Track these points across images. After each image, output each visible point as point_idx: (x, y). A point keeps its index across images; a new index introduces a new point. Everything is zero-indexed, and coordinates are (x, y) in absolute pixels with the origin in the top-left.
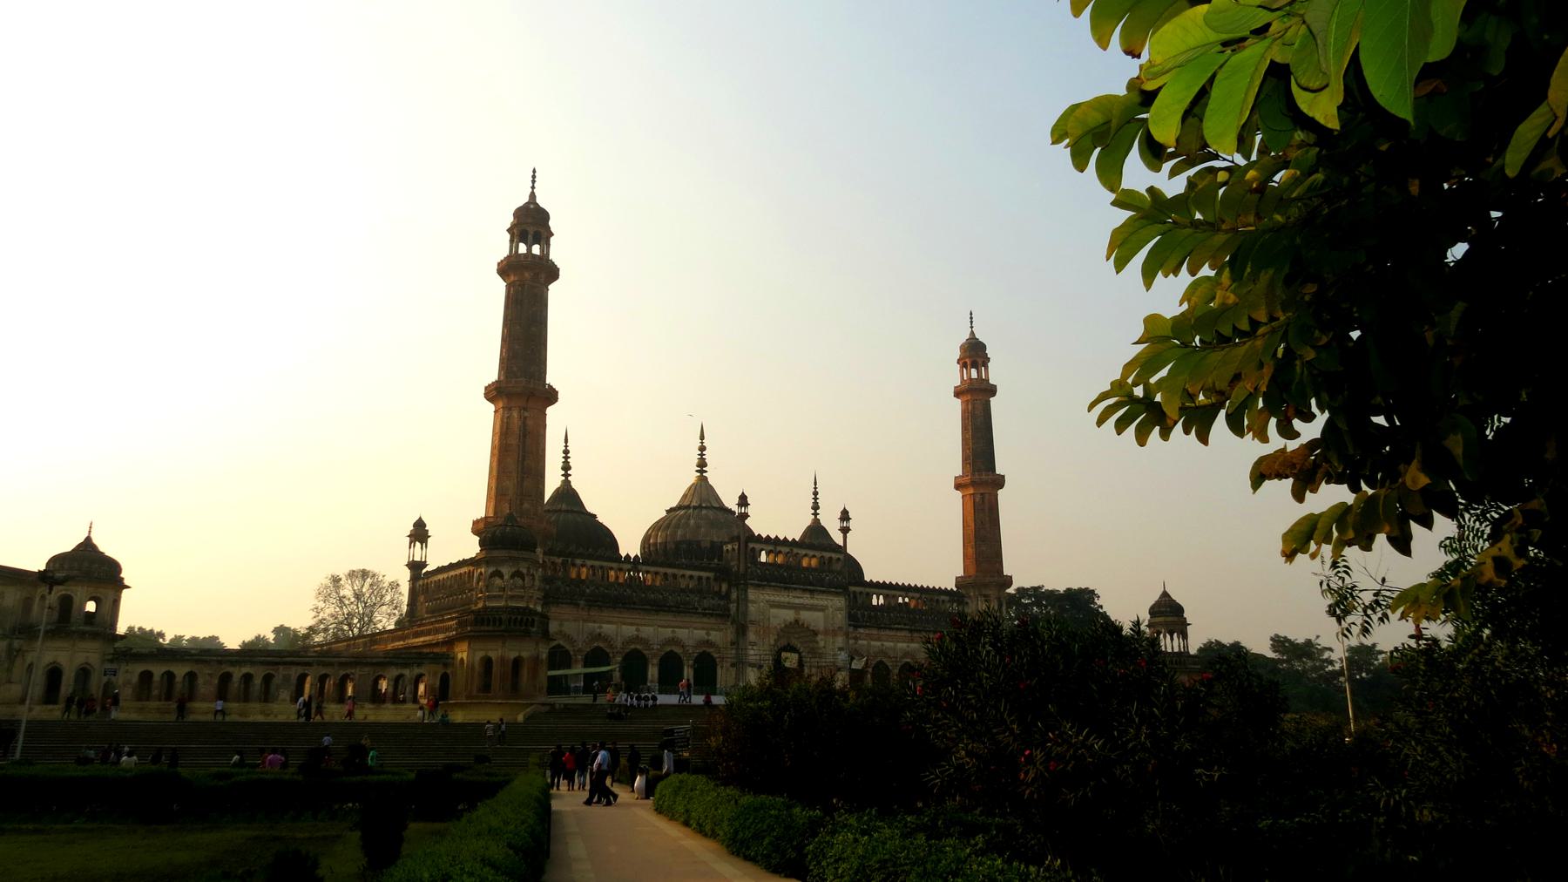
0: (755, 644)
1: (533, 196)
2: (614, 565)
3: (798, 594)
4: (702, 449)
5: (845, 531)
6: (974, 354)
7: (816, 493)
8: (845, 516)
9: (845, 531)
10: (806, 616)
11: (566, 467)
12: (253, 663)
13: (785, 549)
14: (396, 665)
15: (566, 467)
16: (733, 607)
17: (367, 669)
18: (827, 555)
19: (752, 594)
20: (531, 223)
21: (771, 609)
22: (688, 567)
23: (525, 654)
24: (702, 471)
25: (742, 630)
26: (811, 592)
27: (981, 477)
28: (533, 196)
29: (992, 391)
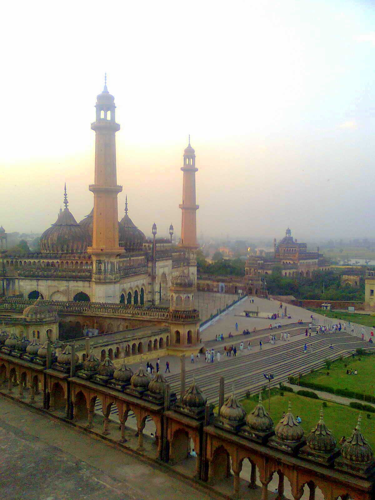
0: (157, 284)
1: (106, 87)
2: (126, 259)
3: (165, 261)
5: (171, 234)
9: (171, 234)
12: (112, 344)
13: (162, 245)
14: (154, 335)
16: (150, 270)
17: (146, 339)
18: (169, 244)
20: (106, 103)
26: (166, 260)
28: (106, 87)
29: (197, 170)
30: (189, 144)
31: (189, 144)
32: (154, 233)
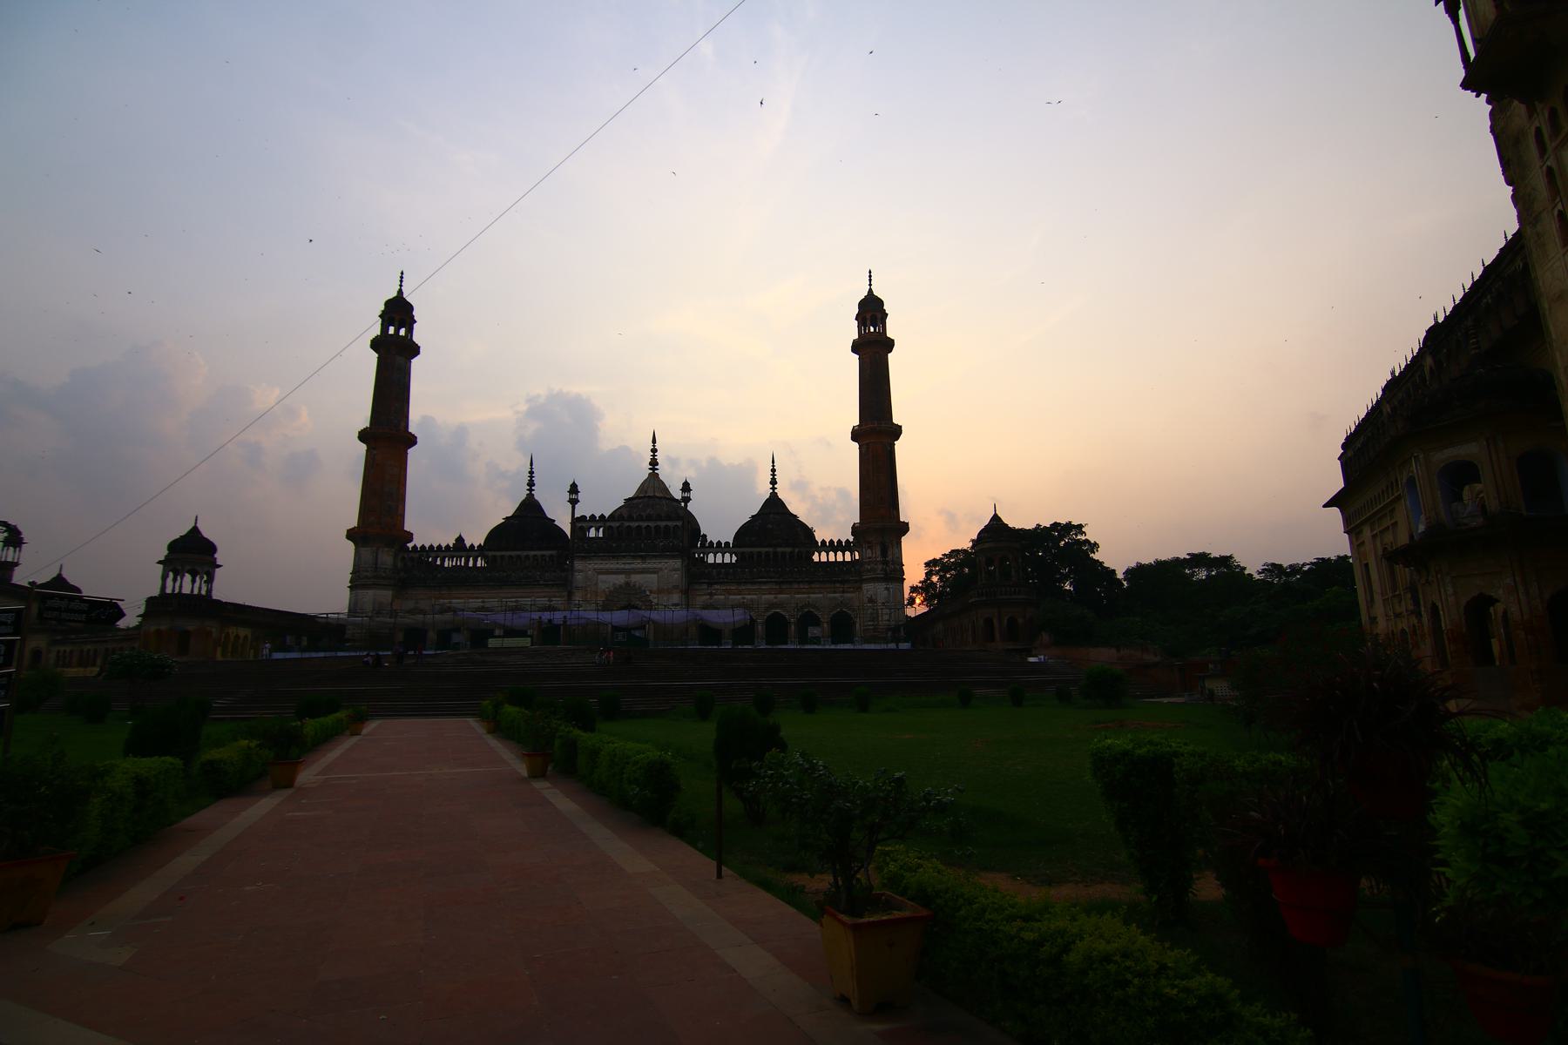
1: (400, 292)
4: (654, 451)
6: (871, 311)
7: (773, 470)
8: (686, 487)
10: (635, 578)
11: (531, 484)
15: (531, 484)
18: (663, 524)
19: (578, 565)
21: (600, 575)
22: (532, 549)
23: (163, 628)
24: (654, 469)
25: (570, 594)
26: (643, 558)
27: (877, 432)
30: (870, 291)
31: (870, 291)
32: (574, 502)
